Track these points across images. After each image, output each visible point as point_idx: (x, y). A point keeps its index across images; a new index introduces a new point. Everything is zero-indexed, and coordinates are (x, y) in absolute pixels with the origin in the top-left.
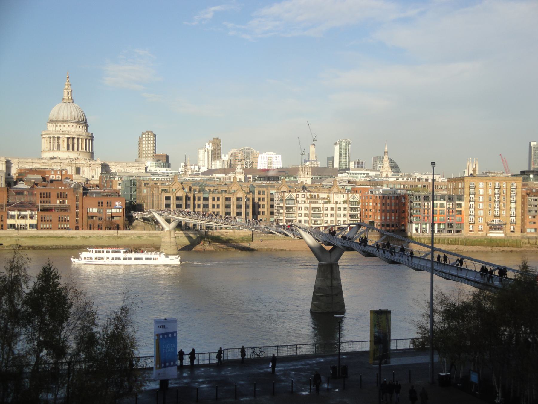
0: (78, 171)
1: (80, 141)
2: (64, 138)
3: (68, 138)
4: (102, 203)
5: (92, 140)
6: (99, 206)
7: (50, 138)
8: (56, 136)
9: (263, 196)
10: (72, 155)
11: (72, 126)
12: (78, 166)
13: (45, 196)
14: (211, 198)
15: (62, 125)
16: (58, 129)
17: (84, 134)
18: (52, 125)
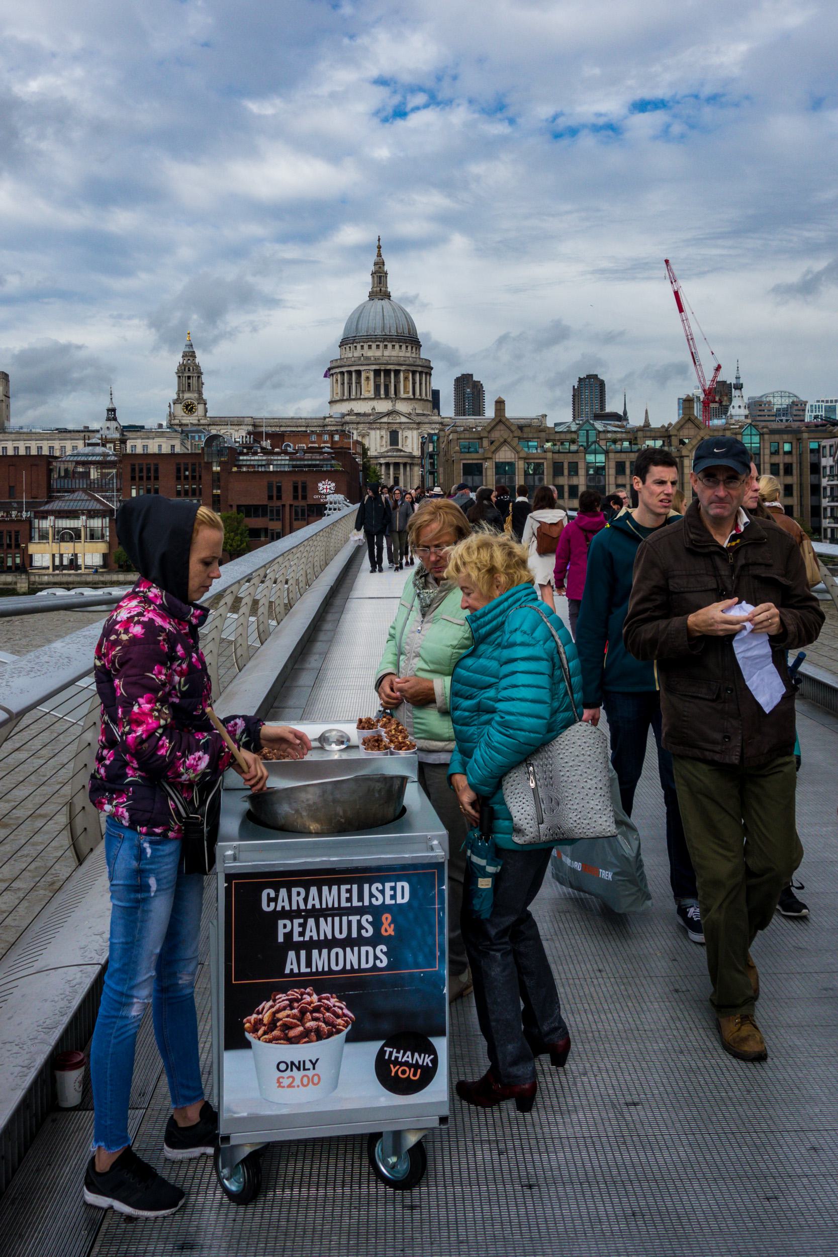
0: (394, 438)
1: (402, 374)
2: (368, 371)
3: (377, 373)
4: (279, 489)
5: (430, 375)
6: (270, 498)
7: (342, 373)
8: (353, 369)
9: (788, 459)
10: (383, 406)
11: (386, 346)
12: (394, 427)
13: (144, 474)
14: (612, 464)
15: (366, 346)
16: (356, 354)
17: (411, 361)
18: (347, 347)
